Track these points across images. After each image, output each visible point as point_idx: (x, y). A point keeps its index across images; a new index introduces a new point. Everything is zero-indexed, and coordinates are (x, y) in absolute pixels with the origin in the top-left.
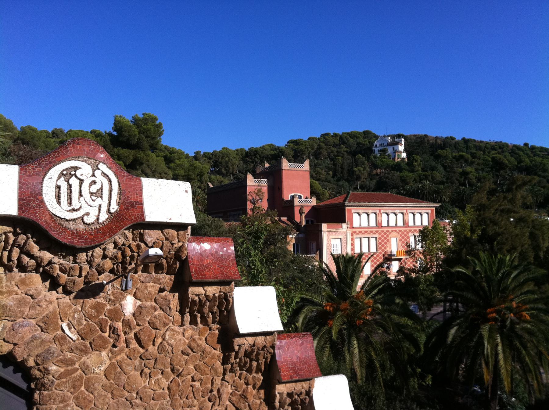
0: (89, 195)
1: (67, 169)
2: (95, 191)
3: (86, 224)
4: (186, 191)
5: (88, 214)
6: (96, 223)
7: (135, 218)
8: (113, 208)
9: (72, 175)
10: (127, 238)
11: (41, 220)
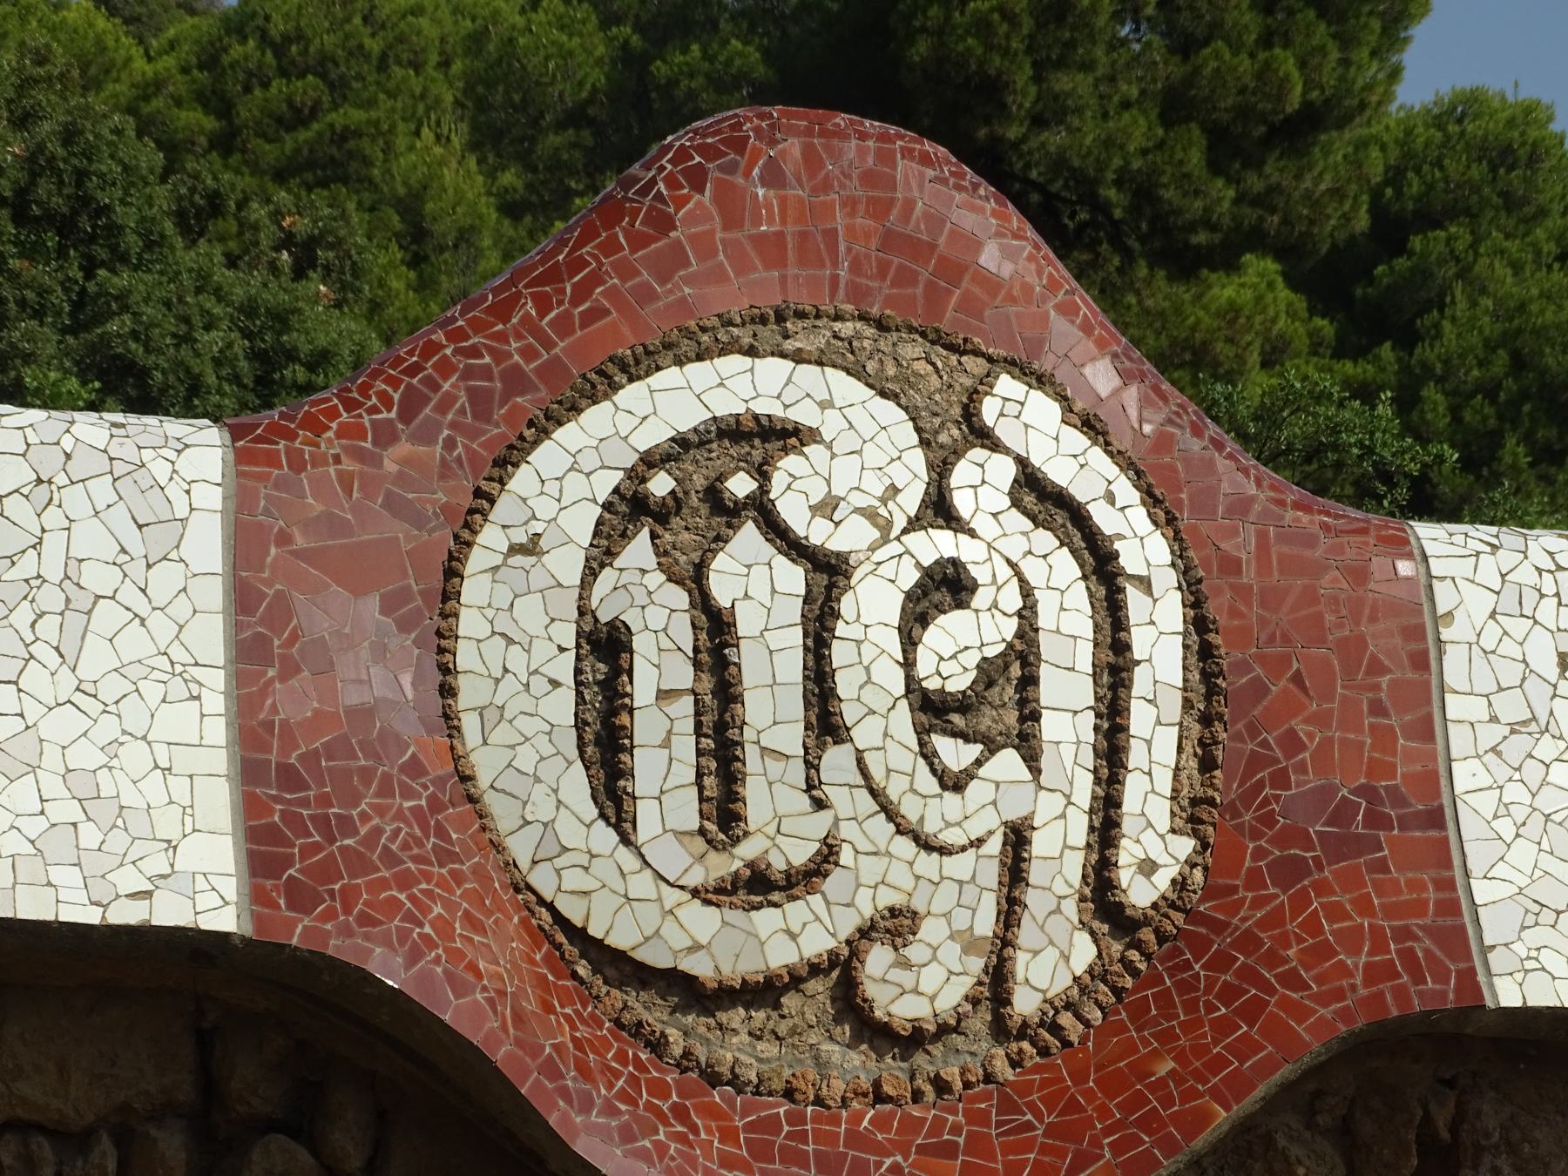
0: (903, 721)
2: (959, 683)
5: (896, 925)
6: (979, 1022)
7: (1374, 974)
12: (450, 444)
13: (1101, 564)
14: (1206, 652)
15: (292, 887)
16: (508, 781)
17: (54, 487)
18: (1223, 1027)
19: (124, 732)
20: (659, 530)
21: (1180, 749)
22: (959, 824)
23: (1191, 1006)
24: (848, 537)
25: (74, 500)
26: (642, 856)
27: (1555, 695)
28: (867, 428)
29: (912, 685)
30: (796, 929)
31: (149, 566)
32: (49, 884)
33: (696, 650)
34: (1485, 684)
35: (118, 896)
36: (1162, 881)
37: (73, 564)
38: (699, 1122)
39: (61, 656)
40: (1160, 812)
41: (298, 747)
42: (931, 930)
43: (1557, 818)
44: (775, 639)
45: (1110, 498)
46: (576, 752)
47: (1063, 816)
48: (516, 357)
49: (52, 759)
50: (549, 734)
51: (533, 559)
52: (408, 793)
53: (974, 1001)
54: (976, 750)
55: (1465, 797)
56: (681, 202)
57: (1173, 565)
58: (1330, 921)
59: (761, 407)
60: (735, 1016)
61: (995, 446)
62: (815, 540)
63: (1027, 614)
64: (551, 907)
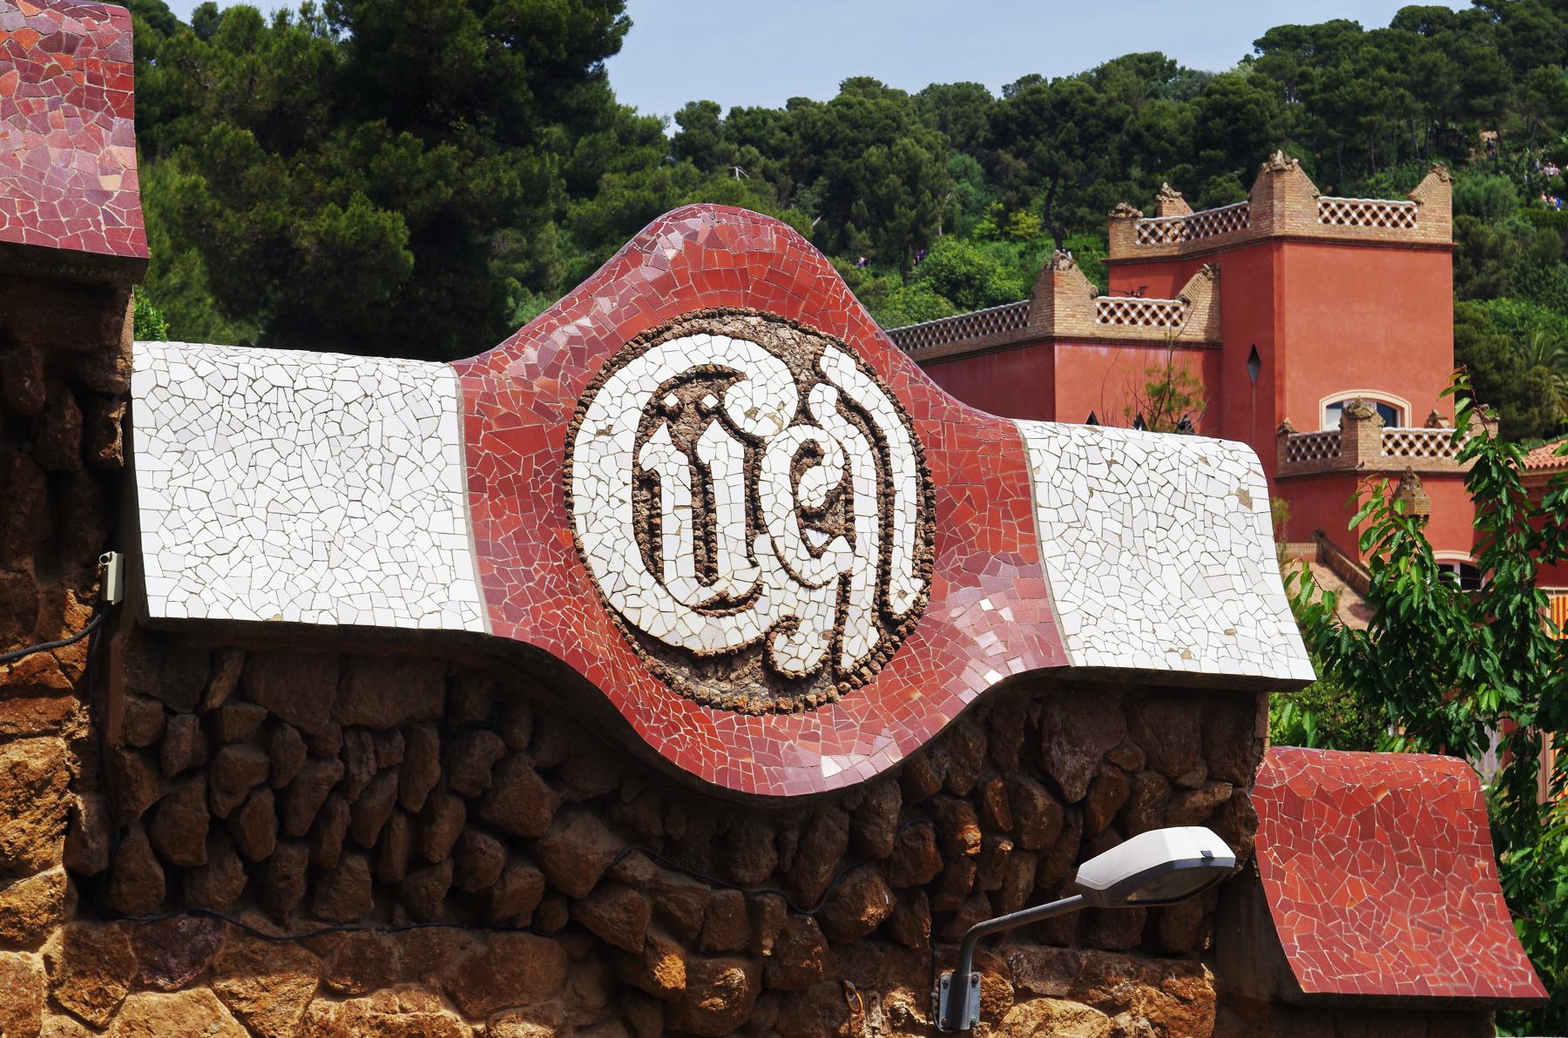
0: (793, 522)
1: (682, 381)
2: (818, 503)
3: (781, 677)
4: (1245, 498)
5: (789, 625)
8: (903, 594)
9: (705, 415)
12: (564, 377)
13: (878, 441)
14: (926, 486)
15: (507, 608)
16: (600, 551)
23: (927, 664)
29: (797, 506)
40: (908, 567)
42: (804, 627)
52: (556, 559)
53: (823, 662)
54: (826, 537)
59: (718, 361)
62: (748, 430)
63: (846, 469)
64: (621, 615)
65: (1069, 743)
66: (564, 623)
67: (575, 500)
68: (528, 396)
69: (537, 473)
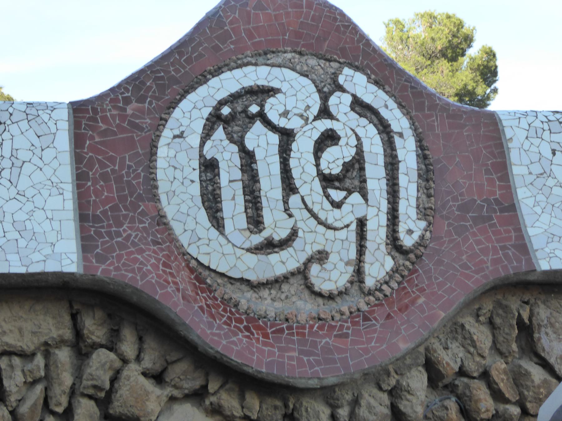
0: (317, 185)
1: (234, 98)
2: (336, 170)
3: (320, 295)
5: (321, 257)
7: (495, 262)
9: (252, 118)
10: (473, 344)
11: (162, 287)
12: (150, 103)
13: (384, 128)
15: (98, 255)
17: (6, 125)
18: (440, 285)
19: (35, 207)
20: (226, 126)
21: (418, 191)
22: (340, 220)
23: (429, 278)
24: (293, 123)
25: (14, 129)
26: (227, 239)
27: (552, 164)
28: (298, 87)
30: (284, 260)
31: (42, 150)
32: (7, 260)
33: (242, 165)
34: (526, 161)
35: (32, 263)
36: (416, 236)
37: (14, 152)
38: (254, 331)
39: (11, 183)
41: (100, 208)
42: (333, 258)
43: (557, 205)
44: (269, 160)
45: (386, 106)
46: (202, 204)
47: (377, 215)
48: (173, 73)
49: (8, 218)
50: (192, 199)
51: (182, 139)
52: (141, 222)
53: (352, 282)
54: (344, 193)
55: (523, 200)
56: (227, 17)
57: (411, 128)
58: (477, 245)
59: (261, 83)
60: (265, 293)
61: (343, 90)
62: (282, 125)
64: (196, 260)
65: (555, 333)
66: (141, 263)
67: (159, 183)
68: (123, 118)
69: (129, 167)
